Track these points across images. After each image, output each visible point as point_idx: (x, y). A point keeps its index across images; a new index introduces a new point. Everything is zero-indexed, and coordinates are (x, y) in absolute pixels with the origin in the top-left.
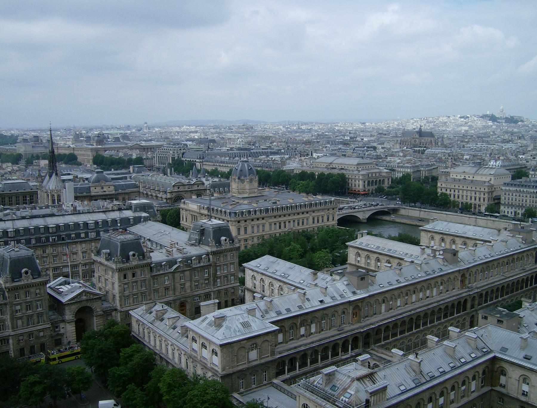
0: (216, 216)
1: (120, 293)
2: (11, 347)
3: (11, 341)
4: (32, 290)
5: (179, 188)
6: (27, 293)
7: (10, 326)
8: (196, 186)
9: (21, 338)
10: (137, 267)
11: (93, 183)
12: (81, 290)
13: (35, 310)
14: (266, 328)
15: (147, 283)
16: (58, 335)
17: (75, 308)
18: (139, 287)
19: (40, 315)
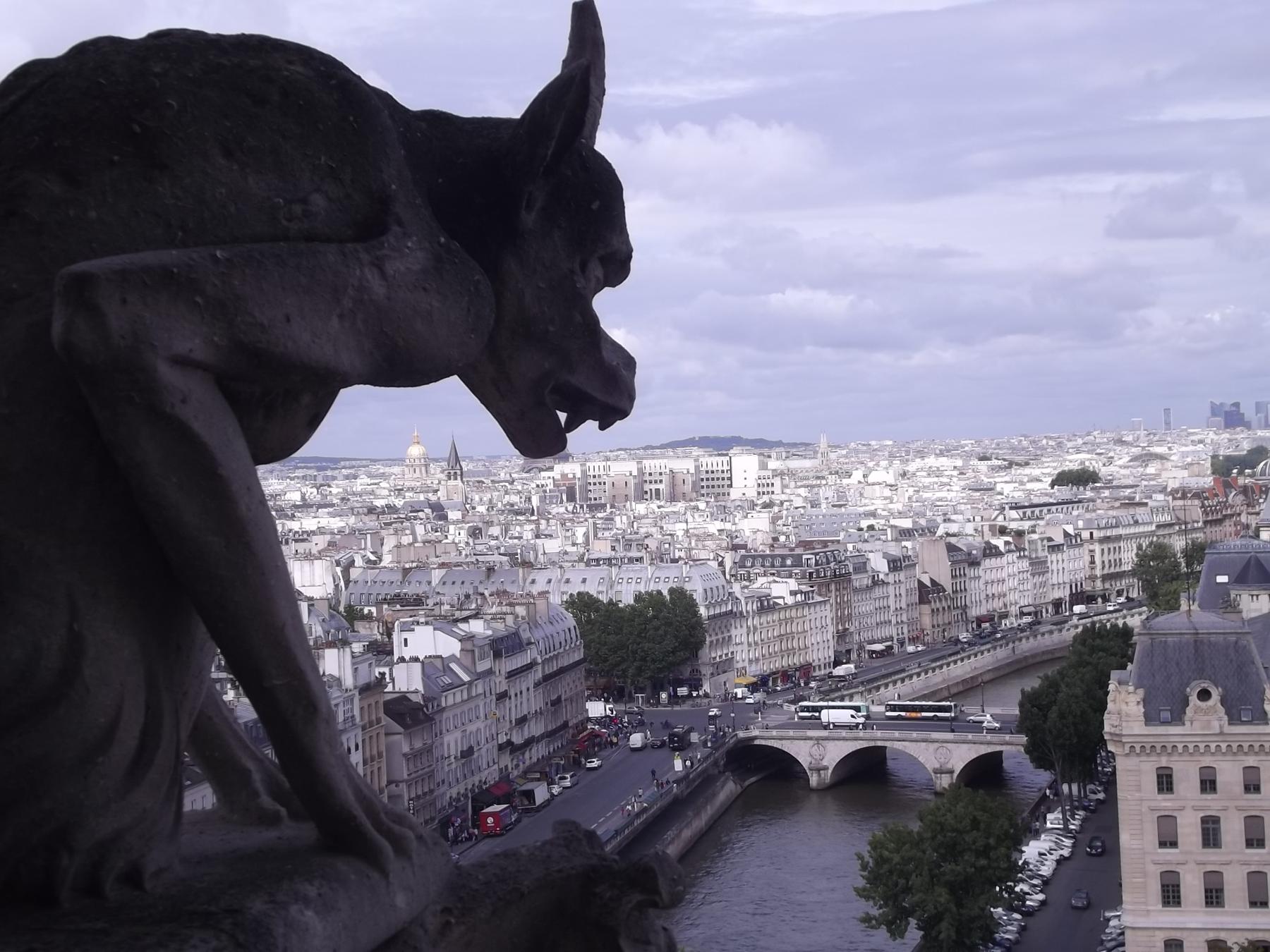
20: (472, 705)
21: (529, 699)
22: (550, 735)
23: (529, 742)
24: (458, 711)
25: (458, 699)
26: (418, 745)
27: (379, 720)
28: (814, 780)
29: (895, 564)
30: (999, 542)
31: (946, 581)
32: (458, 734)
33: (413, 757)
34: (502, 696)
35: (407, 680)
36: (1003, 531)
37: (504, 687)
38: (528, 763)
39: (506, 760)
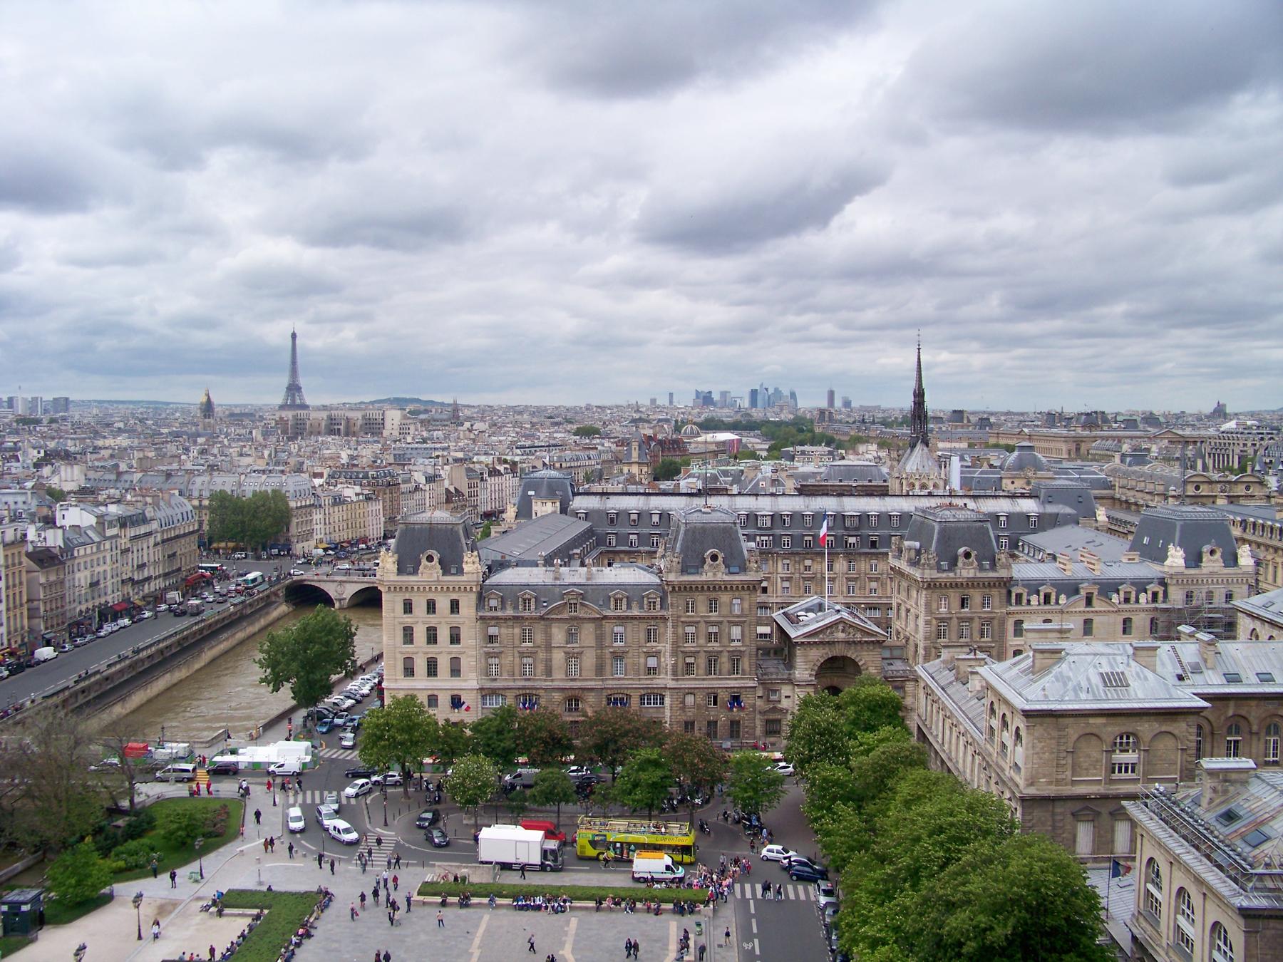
0: (1260, 540)
1: (926, 639)
2: (668, 713)
3: (667, 700)
4: (725, 598)
5: (1197, 488)
6: (713, 604)
7: (669, 667)
8: (1244, 487)
9: (690, 700)
10: (973, 583)
11: (1008, 469)
12: (838, 617)
13: (725, 641)
14: (1171, 699)
15: (996, 628)
16: (774, 710)
17: (818, 655)
18: (976, 636)
19: (736, 657)
20: (101, 556)
21: (148, 552)
22: (166, 575)
23: (148, 579)
24: (88, 559)
25: (89, 551)
26: (53, 578)
27: (20, 563)
28: (337, 605)
29: (431, 479)
30: (501, 468)
31: (466, 491)
32: (88, 573)
33: (49, 586)
34: (127, 550)
35: (54, 539)
36: (506, 462)
37: (129, 545)
38: (146, 591)
39: (128, 589)
